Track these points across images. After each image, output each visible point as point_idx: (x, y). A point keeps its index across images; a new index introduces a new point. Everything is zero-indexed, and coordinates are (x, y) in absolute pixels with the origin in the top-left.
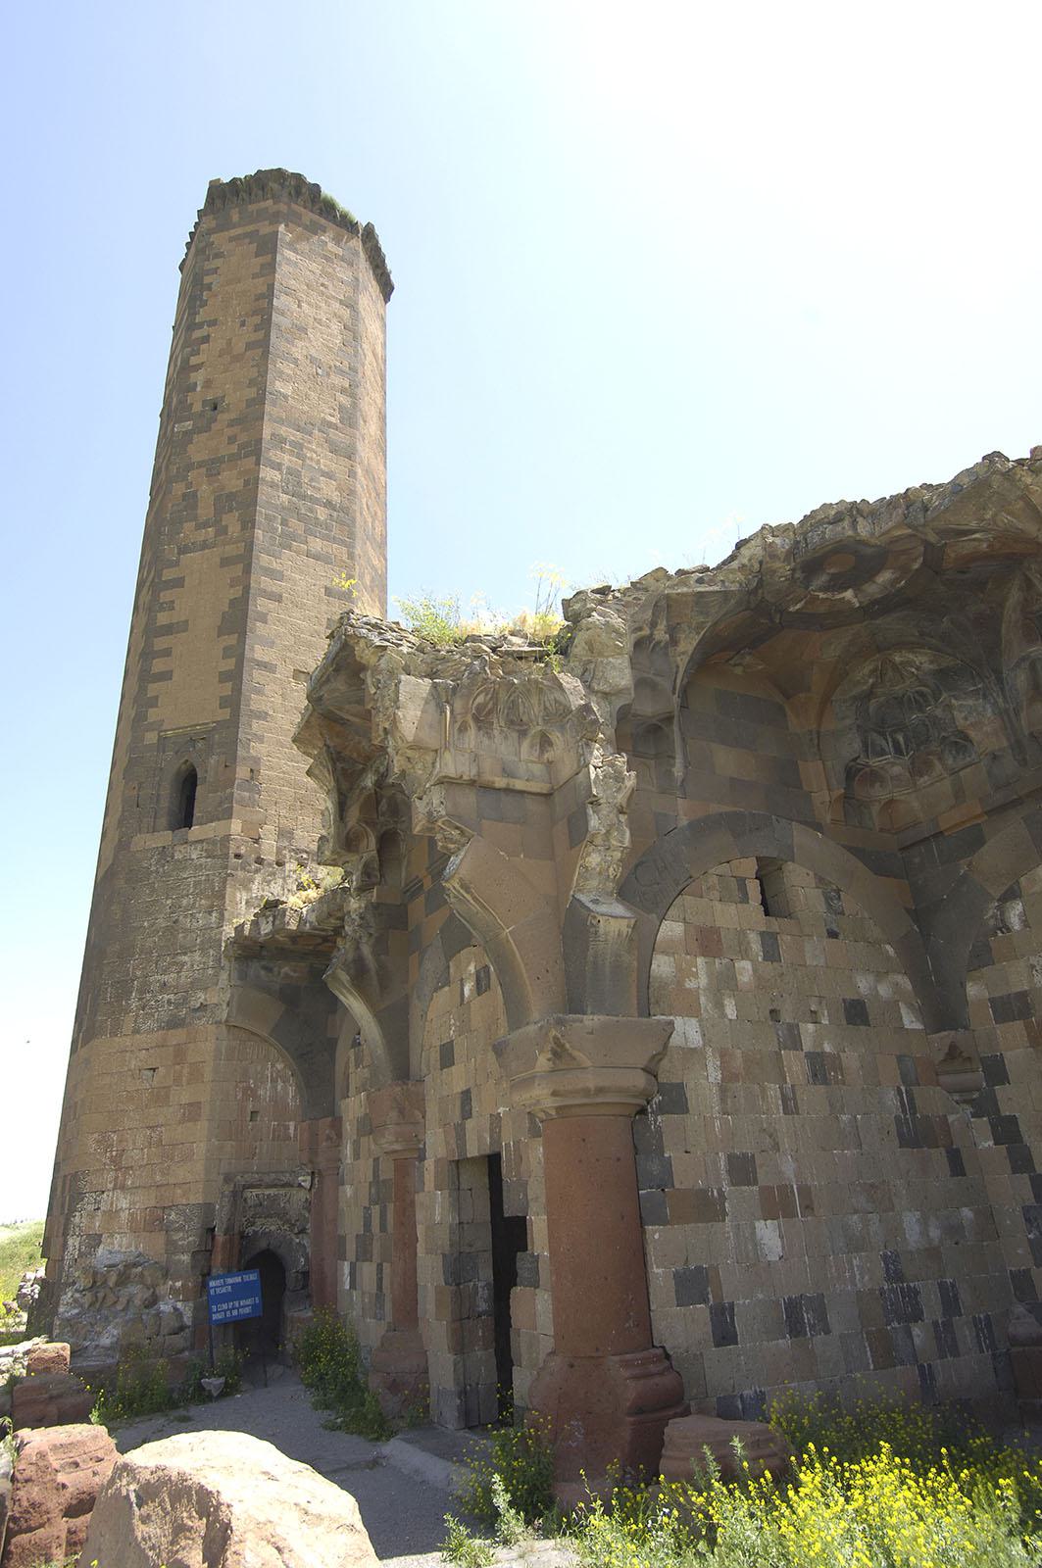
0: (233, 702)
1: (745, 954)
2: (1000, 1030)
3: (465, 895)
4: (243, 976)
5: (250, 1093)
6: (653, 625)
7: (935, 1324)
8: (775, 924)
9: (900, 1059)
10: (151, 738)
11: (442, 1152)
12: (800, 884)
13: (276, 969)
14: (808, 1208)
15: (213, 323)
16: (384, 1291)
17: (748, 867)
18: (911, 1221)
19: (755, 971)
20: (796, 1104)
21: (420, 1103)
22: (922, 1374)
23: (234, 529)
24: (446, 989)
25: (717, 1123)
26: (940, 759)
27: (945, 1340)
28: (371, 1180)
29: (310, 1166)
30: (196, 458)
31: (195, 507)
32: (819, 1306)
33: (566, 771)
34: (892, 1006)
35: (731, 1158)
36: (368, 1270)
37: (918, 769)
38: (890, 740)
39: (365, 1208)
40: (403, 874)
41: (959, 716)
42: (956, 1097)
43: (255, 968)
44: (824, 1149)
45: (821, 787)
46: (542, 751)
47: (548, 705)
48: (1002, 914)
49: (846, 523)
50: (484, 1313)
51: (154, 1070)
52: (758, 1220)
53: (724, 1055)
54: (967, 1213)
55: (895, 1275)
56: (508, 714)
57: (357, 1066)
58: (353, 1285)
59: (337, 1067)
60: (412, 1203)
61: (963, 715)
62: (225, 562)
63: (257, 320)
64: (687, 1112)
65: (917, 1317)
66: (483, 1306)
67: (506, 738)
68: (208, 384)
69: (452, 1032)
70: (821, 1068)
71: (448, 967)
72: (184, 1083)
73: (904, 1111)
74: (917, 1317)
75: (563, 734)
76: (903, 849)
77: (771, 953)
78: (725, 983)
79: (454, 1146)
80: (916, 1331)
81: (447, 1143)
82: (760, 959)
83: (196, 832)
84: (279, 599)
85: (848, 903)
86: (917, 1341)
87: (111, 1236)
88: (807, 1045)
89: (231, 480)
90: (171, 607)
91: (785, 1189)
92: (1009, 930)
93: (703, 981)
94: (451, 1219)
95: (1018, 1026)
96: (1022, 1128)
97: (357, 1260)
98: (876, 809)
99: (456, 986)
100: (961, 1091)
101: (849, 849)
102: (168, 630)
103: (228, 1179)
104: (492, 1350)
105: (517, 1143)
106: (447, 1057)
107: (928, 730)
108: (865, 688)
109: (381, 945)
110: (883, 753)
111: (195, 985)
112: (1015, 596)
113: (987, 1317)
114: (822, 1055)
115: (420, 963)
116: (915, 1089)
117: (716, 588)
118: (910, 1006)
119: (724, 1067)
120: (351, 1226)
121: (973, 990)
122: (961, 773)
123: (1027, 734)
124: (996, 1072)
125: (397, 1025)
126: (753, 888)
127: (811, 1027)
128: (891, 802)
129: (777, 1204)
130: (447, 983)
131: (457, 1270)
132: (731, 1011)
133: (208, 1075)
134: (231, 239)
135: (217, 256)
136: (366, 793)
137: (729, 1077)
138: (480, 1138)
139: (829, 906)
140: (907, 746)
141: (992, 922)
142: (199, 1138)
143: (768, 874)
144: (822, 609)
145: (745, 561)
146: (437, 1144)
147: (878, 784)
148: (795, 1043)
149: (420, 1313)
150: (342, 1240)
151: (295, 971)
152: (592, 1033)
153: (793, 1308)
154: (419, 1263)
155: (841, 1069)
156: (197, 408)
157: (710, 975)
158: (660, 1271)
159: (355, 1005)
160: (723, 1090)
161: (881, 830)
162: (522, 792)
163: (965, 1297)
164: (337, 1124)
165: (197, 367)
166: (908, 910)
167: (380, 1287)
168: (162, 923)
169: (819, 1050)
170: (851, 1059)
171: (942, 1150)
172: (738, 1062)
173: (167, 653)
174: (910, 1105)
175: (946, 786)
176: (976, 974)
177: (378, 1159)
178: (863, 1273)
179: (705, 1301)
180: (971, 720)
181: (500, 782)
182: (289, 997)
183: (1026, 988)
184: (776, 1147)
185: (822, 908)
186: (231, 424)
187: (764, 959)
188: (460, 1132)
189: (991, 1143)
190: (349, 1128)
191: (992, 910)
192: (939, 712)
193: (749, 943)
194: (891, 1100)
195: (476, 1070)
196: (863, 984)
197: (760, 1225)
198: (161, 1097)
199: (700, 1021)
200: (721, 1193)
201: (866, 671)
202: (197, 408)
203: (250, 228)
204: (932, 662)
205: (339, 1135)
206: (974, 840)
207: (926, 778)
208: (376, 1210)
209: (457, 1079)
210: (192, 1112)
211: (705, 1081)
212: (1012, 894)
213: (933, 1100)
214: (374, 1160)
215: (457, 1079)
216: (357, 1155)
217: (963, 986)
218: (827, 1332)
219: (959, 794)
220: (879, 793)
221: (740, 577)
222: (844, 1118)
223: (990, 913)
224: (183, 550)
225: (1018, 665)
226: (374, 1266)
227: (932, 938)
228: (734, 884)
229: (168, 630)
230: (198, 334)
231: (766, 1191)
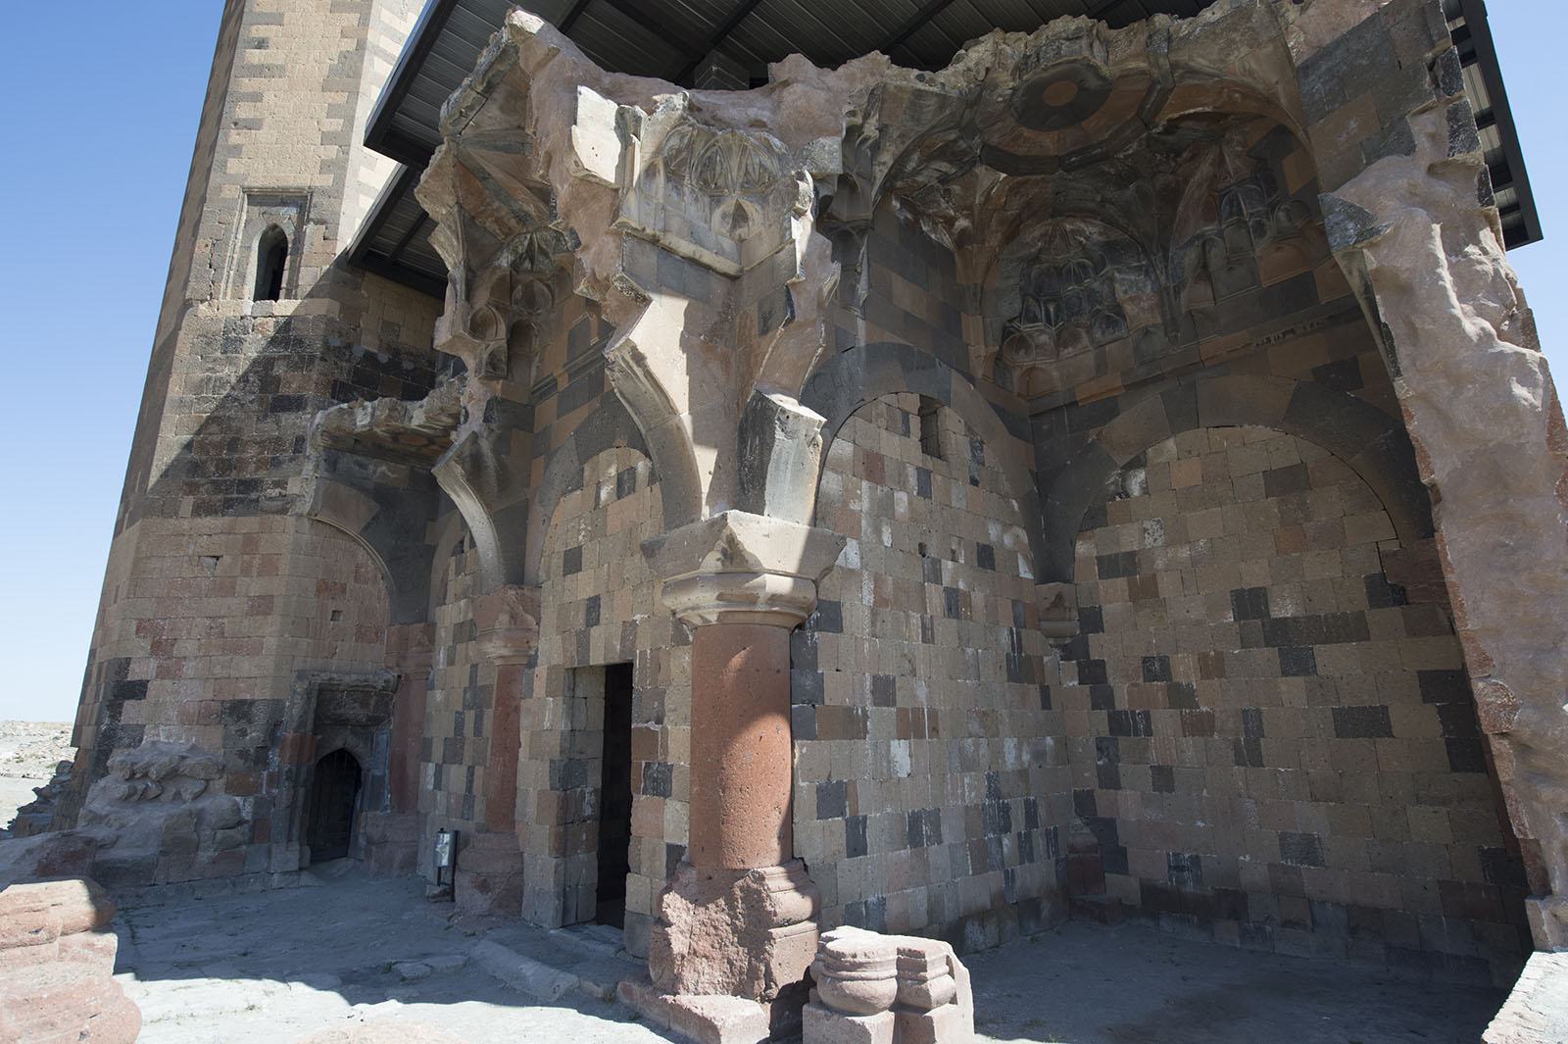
1: (903, 487)
2: (1104, 585)
3: (635, 368)
6: (866, 116)
7: (1019, 834)
8: (930, 463)
9: (1015, 603)
11: (557, 659)
12: (953, 426)
13: (371, 467)
14: (934, 730)
16: (475, 792)
17: (912, 402)
18: (1010, 744)
19: (910, 503)
20: (932, 634)
21: (535, 609)
22: (1007, 878)
24: (579, 492)
25: (867, 645)
26: (1087, 332)
27: (1025, 851)
28: (467, 685)
29: (397, 669)
32: (935, 817)
33: (763, 250)
34: (1012, 555)
35: (876, 679)
36: (456, 775)
37: (1061, 342)
38: (1043, 308)
39: (457, 712)
40: (534, 373)
41: (1119, 289)
42: (1051, 641)
43: (347, 462)
44: (951, 678)
45: (979, 342)
46: (734, 227)
47: (750, 169)
48: (1124, 480)
49: (1084, 42)
50: (589, 818)
51: (217, 558)
52: (894, 739)
53: (878, 580)
54: (1049, 741)
55: (994, 793)
56: (701, 172)
57: (458, 573)
58: (438, 786)
59: (433, 575)
60: (517, 709)
61: (1124, 288)
64: (842, 631)
65: (1007, 829)
66: (588, 811)
67: (696, 199)
69: (581, 538)
71: (582, 470)
72: (254, 572)
73: (1013, 650)
74: (1007, 829)
75: (763, 208)
76: (1034, 416)
77: (925, 490)
78: (883, 510)
79: (574, 653)
80: (1005, 841)
81: (565, 650)
82: (915, 493)
85: (988, 454)
86: (1005, 850)
87: (157, 726)
88: (946, 581)
91: (918, 711)
92: (1128, 496)
93: (866, 505)
94: (563, 725)
95: (1121, 583)
96: (1109, 671)
97: (444, 762)
98: (1017, 373)
99: (590, 491)
100: (1056, 637)
101: (993, 406)
103: (301, 675)
104: (594, 854)
105: (656, 650)
106: (573, 562)
107: (1081, 303)
108: (1033, 250)
109: (501, 444)
110: (1035, 319)
112: (1205, 169)
113: (1055, 829)
114: (957, 590)
115: (546, 468)
116: (1023, 632)
117: (935, 89)
118: (1026, 557)
119: (877, 591)
120: (440, 729)
121: (1082, 548)
122: (1107, 348)
123: (1183, 312)
124: (1092, 620)
125: (513, 526)
126: (915, 423)
127: (950, 563)
128: (1032, 369)
129: (911, 726)
130: (579, 486)
131: (566, 775)
133: (284, 566)
136: (499, 273)
137: (880, 602)
138: (608, 647)
139: (974, 456)
140: (1057, 317)
141: (1113, 488)
142: (270, 632)
143: (929, 411)
144: (1021, 151)
145: (971, 65)
146: (551, 650)
147: (1022, 352)
148: (937, 578)
149: (517, 817)
150: (427, 744)
151: (393, 473)
152: (768, 536)
153: (915, 820)
154: (520, 766)
155: (971, 607)
157: (872, 500)
158: (805, 784)
159: (470, 507)
160: (874, 613)
161: (1019, 395)
162: (708, 268)
163: (1042, 811)
164: (430, 629)
166: (1031, 471)
167: (469, 788)
169: (954, 587)
170: (978, 598)
171: (1037, 686)
172: (889, 588)
173: (256, 97)
174: (1017, 645)
175: (1089, 359)
176: (1089, 533)
177: (477, 665)
178: (970, 790)
179: (842, 814)
180: (1131, 294)
181: (685, 247)
182: (383, 496)
183: (1135, 548)
184: (913, 672)
185: (968, 455)
187: (918, 494)
188: (583, 642)
189: (1076, 683)
190: (444, 634)
191: (1114, 476)
192: (1096, 285)
193: (907, 476)
194: (1004, 638)
195: (609, 576)
196: (993, 531)
197: (894, 743)
198: (226, 588)
199: (860, 544)
200: (864, 711)
201: (1037, 234)
204: (1101, 234)
205: (432, 641)
206: (1108, 410)
207: (1070, 349)
208: (470, 717)
209: (584, 585)
210: (262, 606)
211: (859, 603)
212: (1137, 463)
213: (1034, 642)
214: (473, 666)
215: (584, 585)
216: (451, 662)
217: (1073, 544)
218: (940, 842)
219: (1101, 367)
220: (1024, 360)
221: (962, 83)
222: (970, 651)
223: (1112, 479)
225: (1190, 243)
226: (464, 769)
227: (1049, 500)
228: (899, 416)
231: (902, 713)
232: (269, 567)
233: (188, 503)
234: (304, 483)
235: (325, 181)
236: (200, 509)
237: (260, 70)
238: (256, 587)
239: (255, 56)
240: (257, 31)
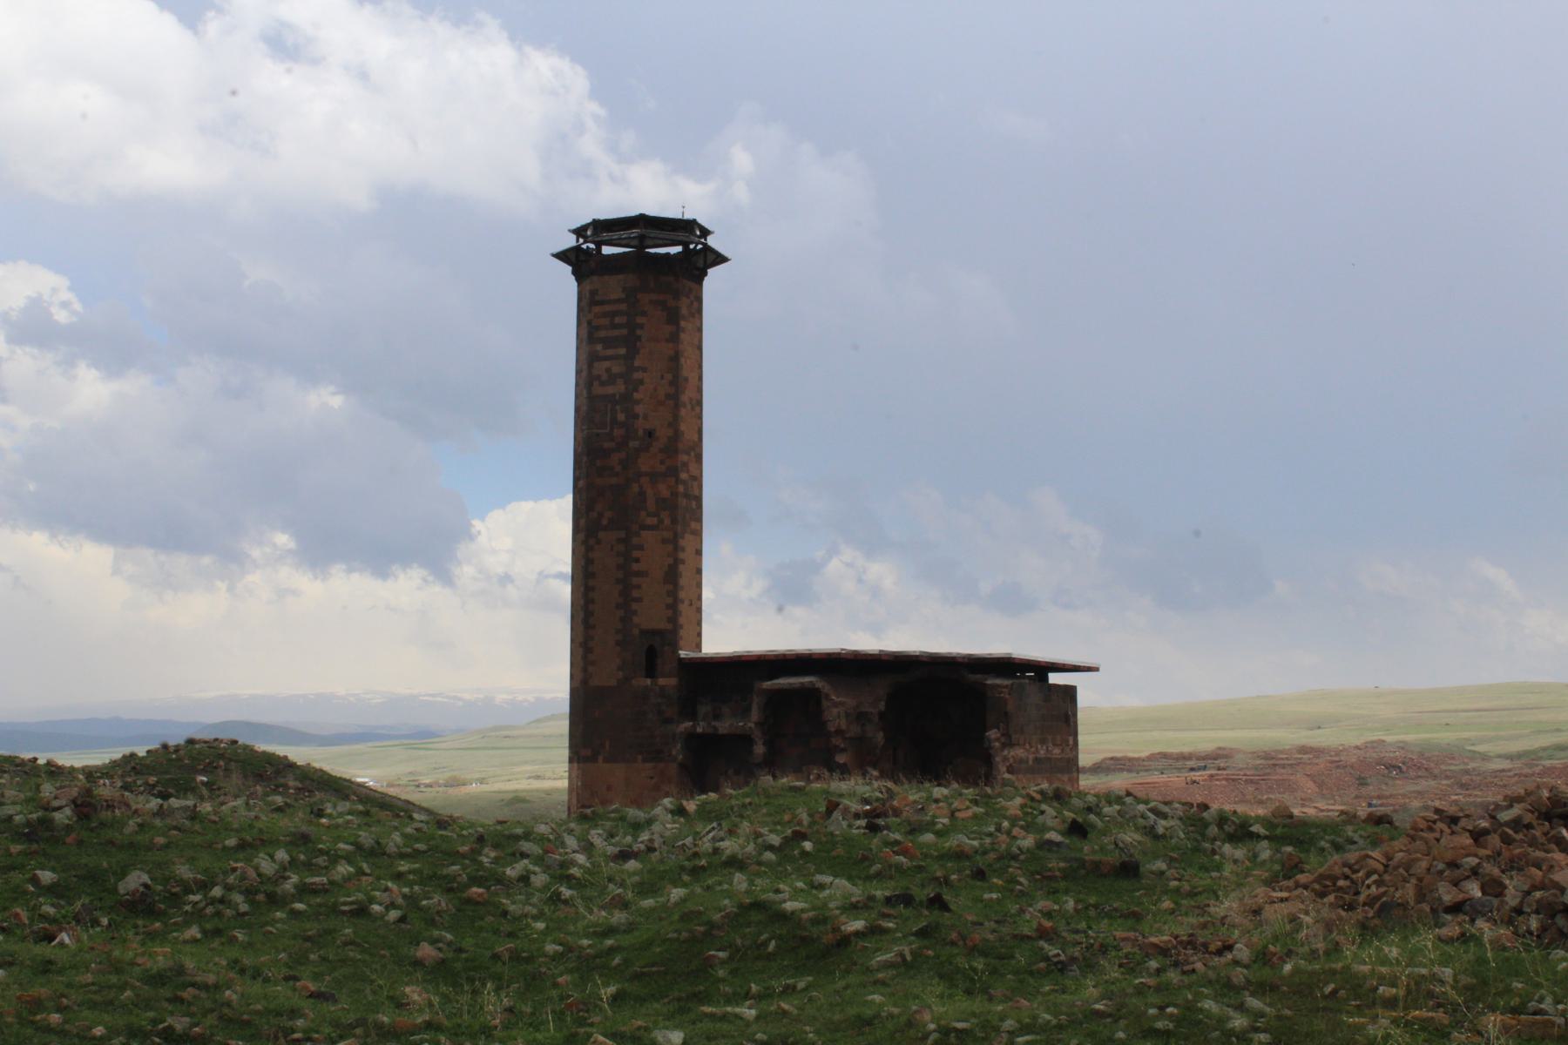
0: (674, 620)
15: (644, 370)
23: (667, 522)
30: (644, 469)
62: (664, 541)
63: (669, 376)
89: (664, 491)
102: (639, 574)
135: (644, 314)
156: (641, 433)
173: (639, 587)
202: (641, 433)
230: (637, 375)
233: (640, 757)
234: (677, 751)
235: (669, 626)
236: (644, 761)
237: (639, 574)
239: (635, 567)
240: (636, 554)
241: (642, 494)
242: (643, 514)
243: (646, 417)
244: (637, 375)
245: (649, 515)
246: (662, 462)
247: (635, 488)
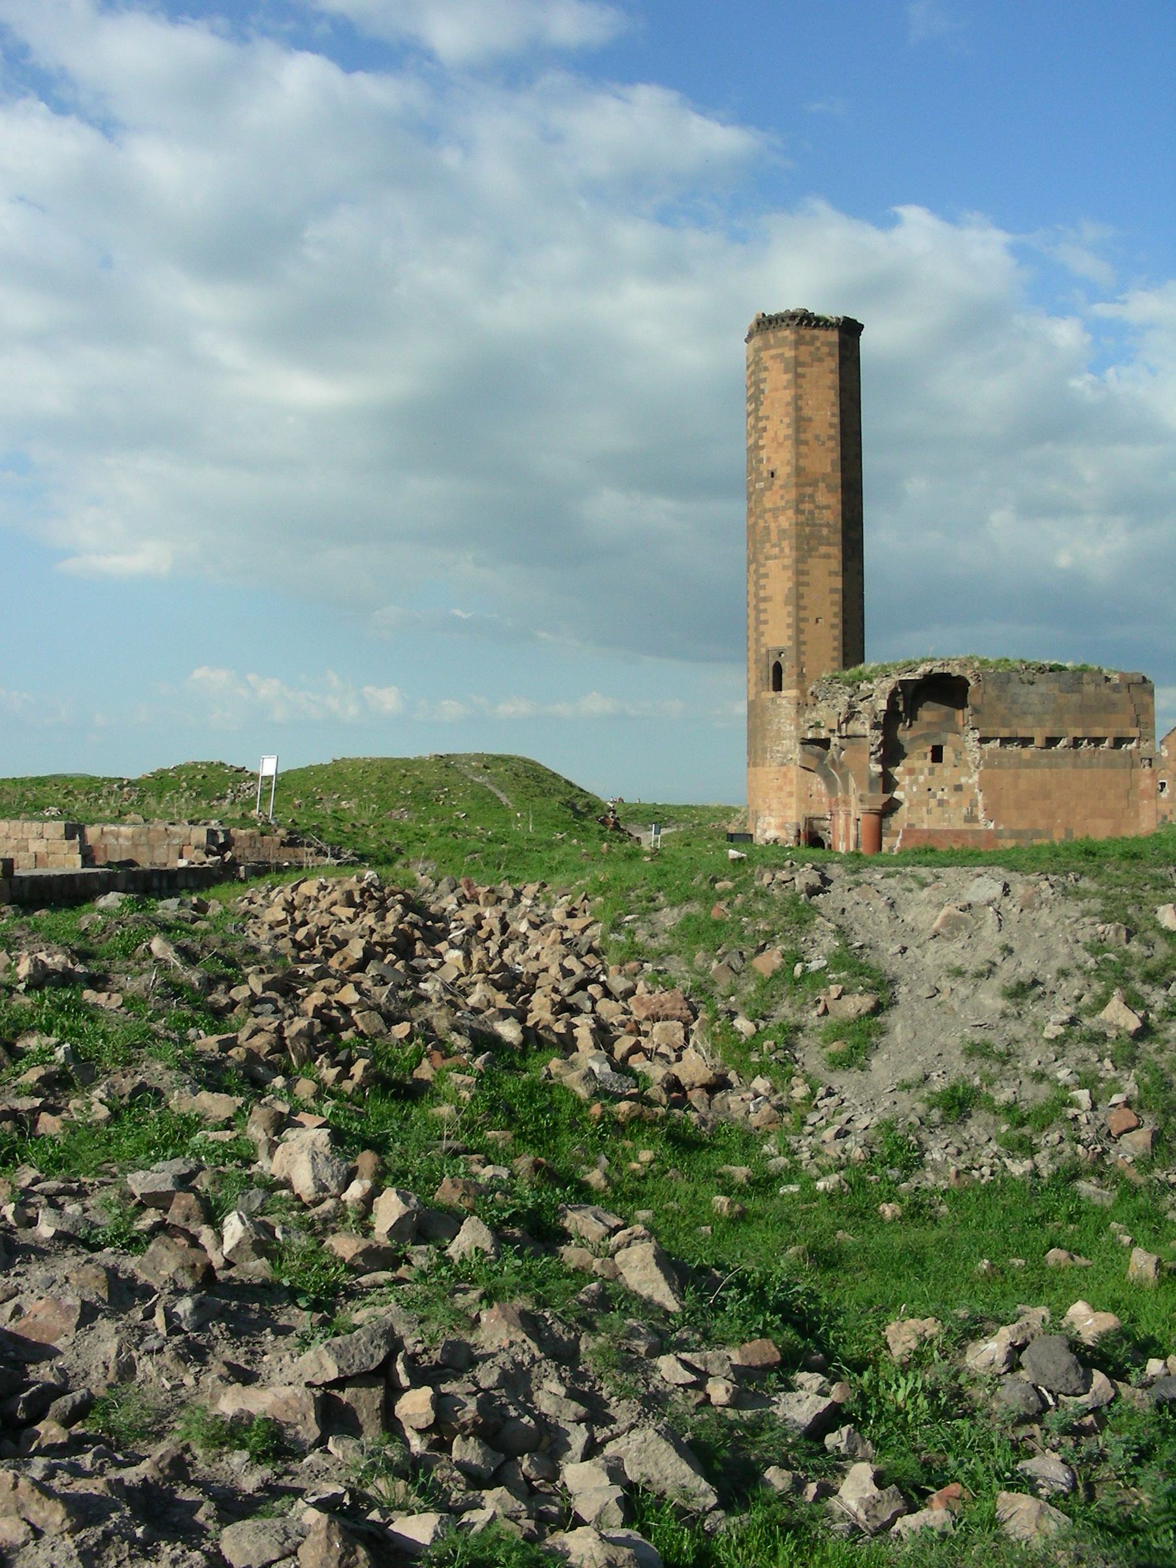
1: (922, 773)
4: (804, 750)
5: (809, 789)
10: (763, 650)
15: (767, 418)
30: (769, 505)
31: (769, 534)
43: (808, 747)
53: (910, 800)
68: (769, 459)
70: (941, 803)
78: (915, 782)
83: (783, 693)
84: (808, 584)
90: (764, 587)
102: (765, 599)
111: (788, 752)
126: (929, 755)
132: (915, 789)
133: (795, 782)
134: (772, 357)
135: (766, 369)
137: (911, 805)
142: (793, 801)
148: (934, 796)
165: (763, 447)
168: (775, 728)
170: (953, 800)
172: (915, 801)
173: (765, 611)
186: (782, 487)
194: (964, 811)
198: (780, 789)
202: (765, 474)
203: (779, 351)
210: (791, 794)
224: (767, 558)
229: (765, 599)
230: (761, 424)
232: (791, 782)
238: (788, 789)
241: (767, 528)
242: (768, 545)
243: (769, 459)
244: (761, 424)
245: (774, 546)
246: (782, 497)
247: (761, 523)
